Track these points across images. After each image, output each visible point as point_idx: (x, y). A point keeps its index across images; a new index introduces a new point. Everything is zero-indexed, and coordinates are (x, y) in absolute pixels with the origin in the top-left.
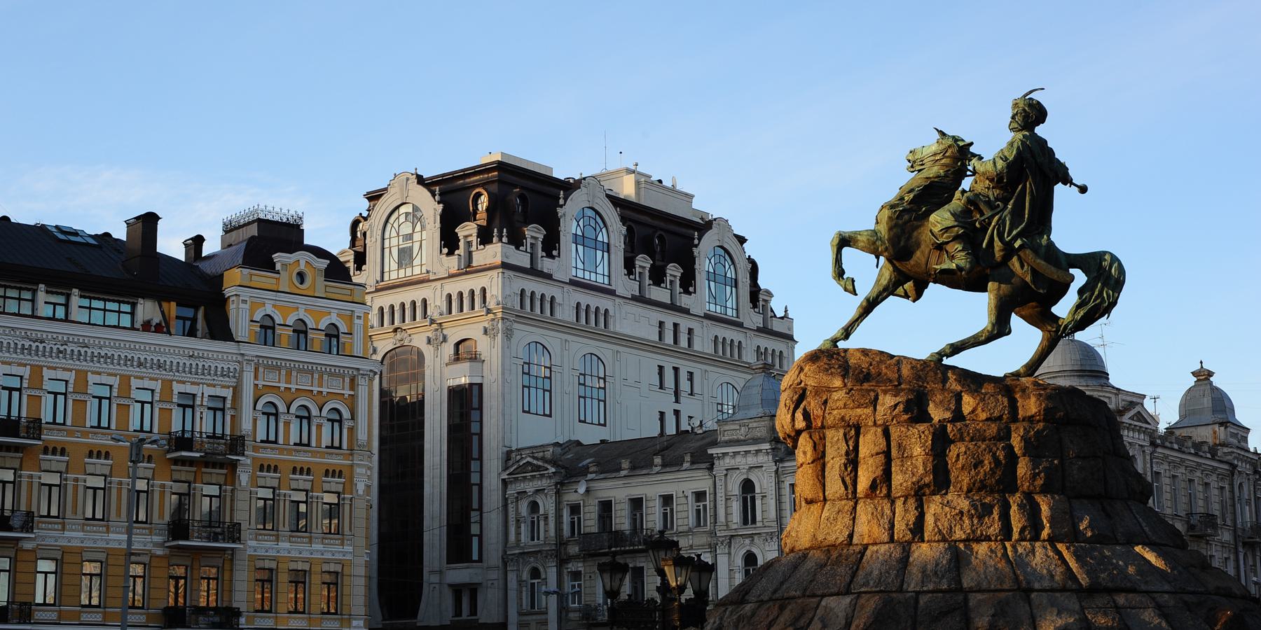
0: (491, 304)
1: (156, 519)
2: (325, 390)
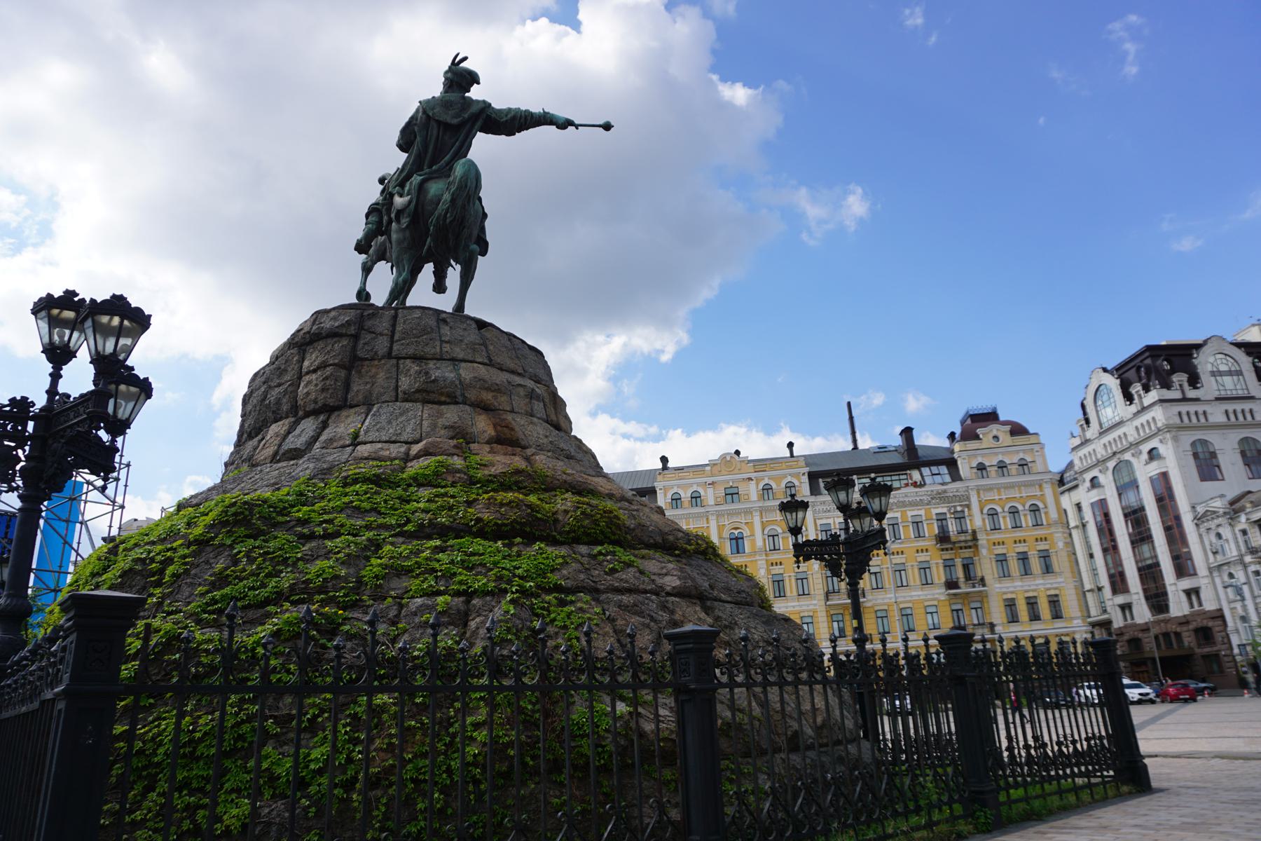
1: (936, 581)
2: (1024, 495)
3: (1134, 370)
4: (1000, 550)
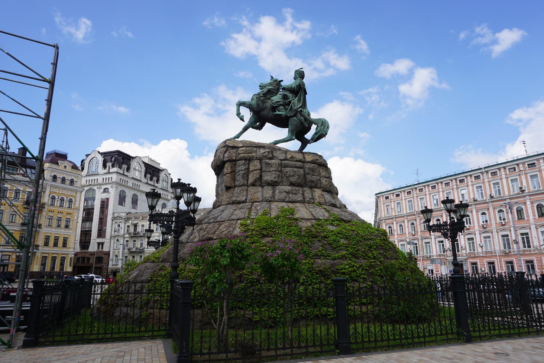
0: (113, 180)
2: (69, 194)
3: (111, 156)
4: (51, 214)
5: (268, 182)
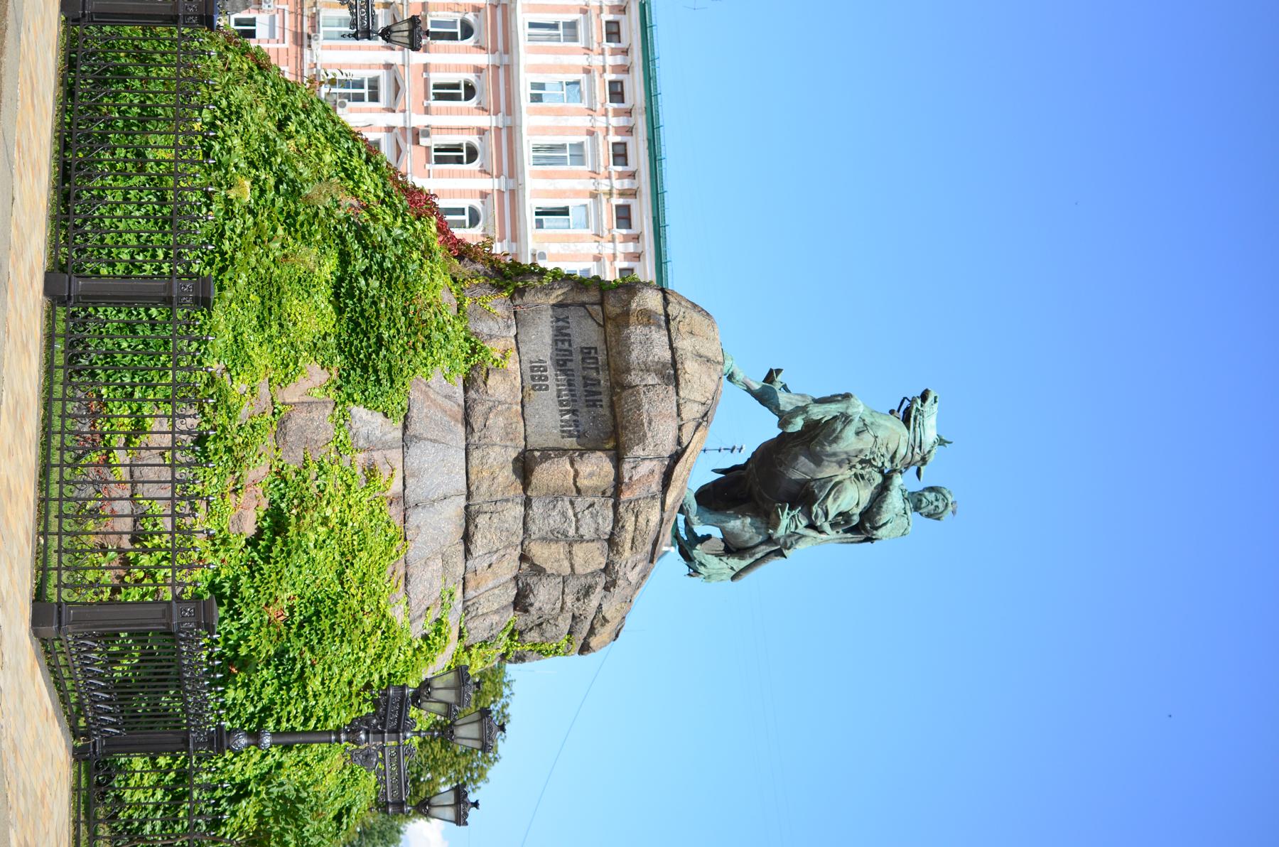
5: (527, 596)
